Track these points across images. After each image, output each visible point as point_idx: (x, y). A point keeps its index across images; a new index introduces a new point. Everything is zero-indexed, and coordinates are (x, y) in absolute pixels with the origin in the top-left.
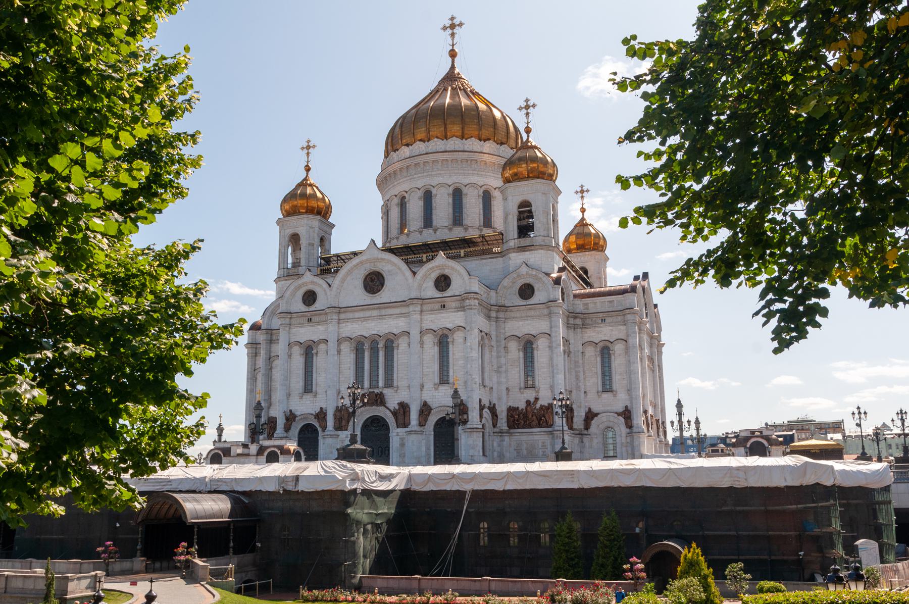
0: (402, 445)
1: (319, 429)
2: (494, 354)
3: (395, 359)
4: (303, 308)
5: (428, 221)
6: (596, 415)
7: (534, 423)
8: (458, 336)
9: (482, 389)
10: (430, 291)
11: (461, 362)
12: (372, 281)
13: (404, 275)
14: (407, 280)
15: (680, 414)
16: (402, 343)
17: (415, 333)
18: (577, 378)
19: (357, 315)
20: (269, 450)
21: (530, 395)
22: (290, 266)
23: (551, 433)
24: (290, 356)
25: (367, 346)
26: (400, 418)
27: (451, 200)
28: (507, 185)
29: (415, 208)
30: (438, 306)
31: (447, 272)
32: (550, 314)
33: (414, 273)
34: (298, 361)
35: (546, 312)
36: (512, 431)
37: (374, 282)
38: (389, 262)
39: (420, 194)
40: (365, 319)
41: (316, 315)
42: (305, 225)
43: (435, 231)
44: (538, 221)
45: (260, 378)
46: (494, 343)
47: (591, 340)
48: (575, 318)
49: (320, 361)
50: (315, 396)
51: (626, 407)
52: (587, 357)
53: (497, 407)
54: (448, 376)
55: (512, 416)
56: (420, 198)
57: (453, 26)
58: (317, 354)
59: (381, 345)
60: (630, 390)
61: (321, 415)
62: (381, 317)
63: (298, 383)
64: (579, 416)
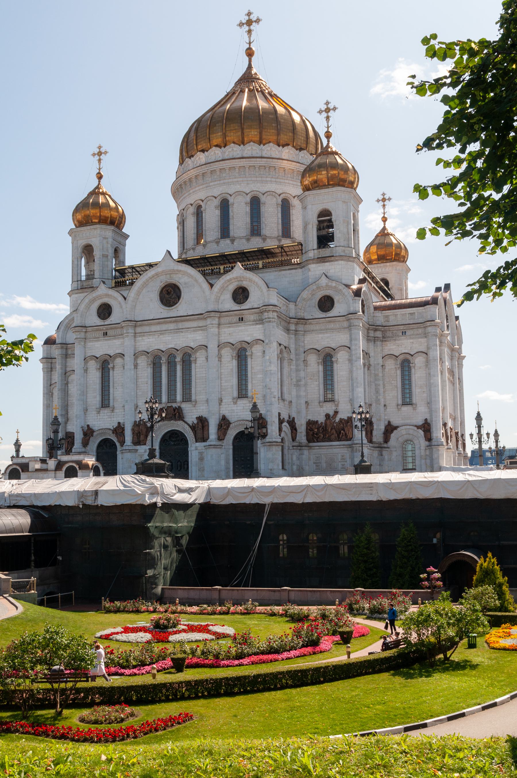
0: (201, 459)
1: (118, 444)
2: (293, 367)
3: (193, 373)
4: (98, 321)
5: (225, 231)
7: (333, 437)
8: (257, 350)
9: (281, 403)
10: (228, 303)
11: (260, 376)
12: (168, 293)
13: (201, 287)
14: (204, 292)
15: (479, 427)
16: (200, 358)
17: (213, 347)
18: (377, 392)
19: (154, 328)
20: (67, 465)
21: (329, 408)
22: (83, 278)
23: (351, 446)
24: (86, 370)
25: (164, 360)
26: (199, 432)
27: (248, 209)
28: (307, 193)
29: (212, 217)
30: (236, 319)
31: (245, 284)
32: (350, 327)
33: (212, 285)
34: (94, 375)
35: (346, 324)
36: (311, 444)
37: (170, 295)
38: (185, 273)
39: (217, 202)
40: (162, 332)
41: (112, 329)
42: (98, 236)
43: (233, 241)
44: (338, 231)
45: (56, 393)
46: (293, 356)
47: (391, 353)
48: (376, 330)
49: (117, 376)
50: (113, 411)
51: (426, 420)
52: (387, 370)
53: (296, 421)
54: (246, 390)
55: (311, 430)
56: (216, 207)
58: (113, 368)
59: (178, 359)
60: (430, 404)
61: (119, 430)
62: (178, 330)
63: (94, 398)
64: (379, 429)
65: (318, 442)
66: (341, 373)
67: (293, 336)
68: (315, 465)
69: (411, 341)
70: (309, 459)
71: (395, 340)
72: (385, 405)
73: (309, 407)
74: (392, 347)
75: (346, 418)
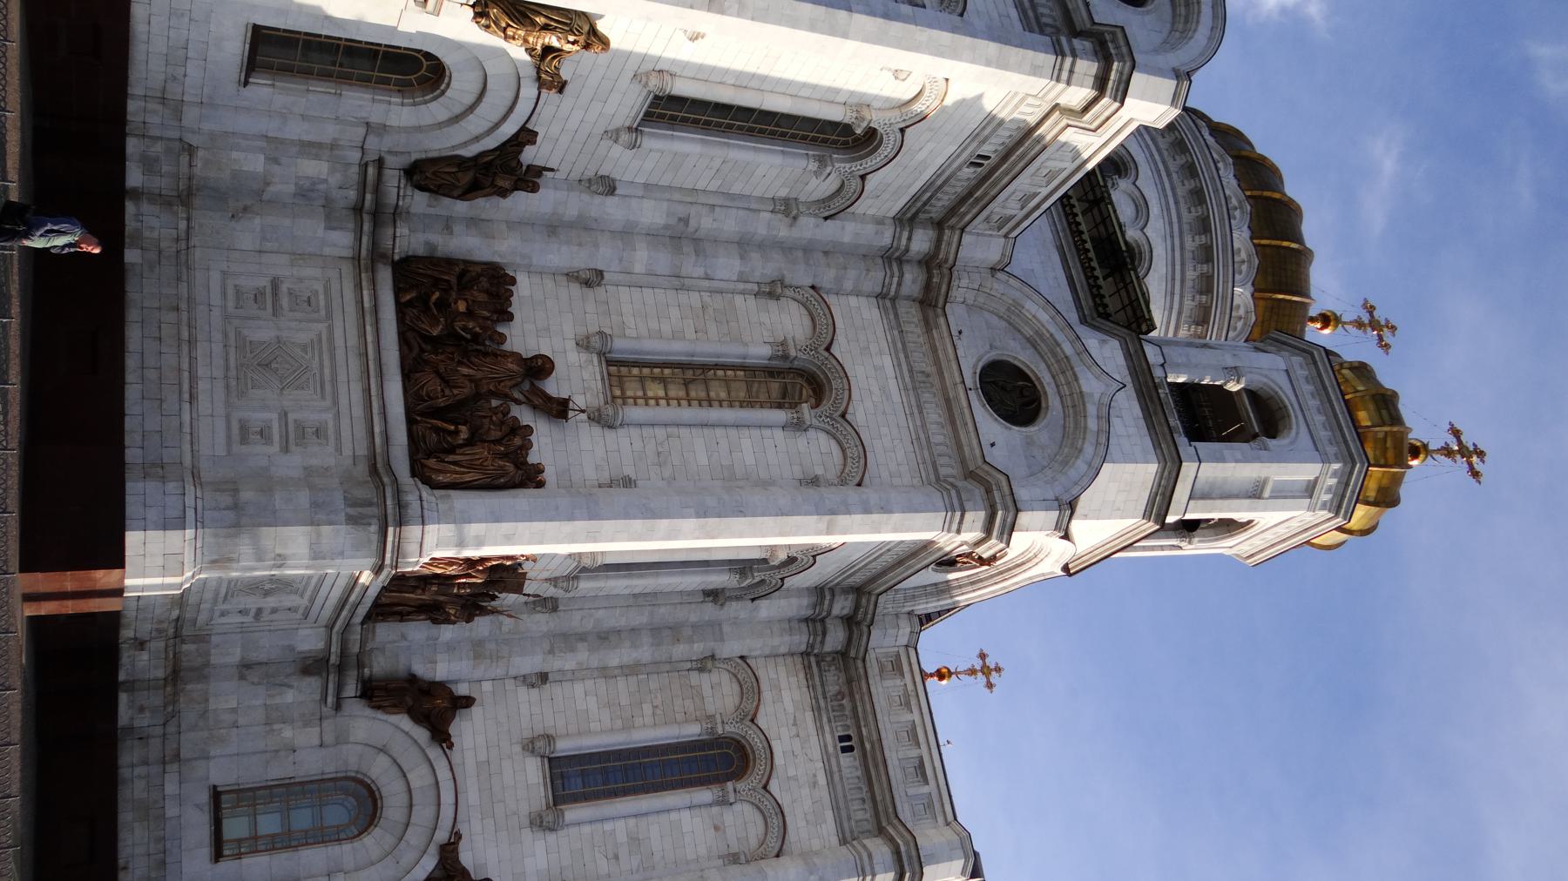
2: (765, 224)
6: (442, 737)
7: (431, 384)
18: (604, 637)
21: (576, 377)
35: (949, 469)
36: (385, 276)
46: (809, 228)
47: (767, 695)
48: (850, 621)
52: (695, 677)
53: (520, 202)
57: (1374, 324)
64: (434, 650)
65: (401, 309)
66: (746, 443)
67: (886, 239)
68: (264, 282)
69: (822, 780)
70: (298, 257)
71: (817, 709)
72: (543, 677)
73: (575, 288)
74: (786, 695)
75: (532, 458)
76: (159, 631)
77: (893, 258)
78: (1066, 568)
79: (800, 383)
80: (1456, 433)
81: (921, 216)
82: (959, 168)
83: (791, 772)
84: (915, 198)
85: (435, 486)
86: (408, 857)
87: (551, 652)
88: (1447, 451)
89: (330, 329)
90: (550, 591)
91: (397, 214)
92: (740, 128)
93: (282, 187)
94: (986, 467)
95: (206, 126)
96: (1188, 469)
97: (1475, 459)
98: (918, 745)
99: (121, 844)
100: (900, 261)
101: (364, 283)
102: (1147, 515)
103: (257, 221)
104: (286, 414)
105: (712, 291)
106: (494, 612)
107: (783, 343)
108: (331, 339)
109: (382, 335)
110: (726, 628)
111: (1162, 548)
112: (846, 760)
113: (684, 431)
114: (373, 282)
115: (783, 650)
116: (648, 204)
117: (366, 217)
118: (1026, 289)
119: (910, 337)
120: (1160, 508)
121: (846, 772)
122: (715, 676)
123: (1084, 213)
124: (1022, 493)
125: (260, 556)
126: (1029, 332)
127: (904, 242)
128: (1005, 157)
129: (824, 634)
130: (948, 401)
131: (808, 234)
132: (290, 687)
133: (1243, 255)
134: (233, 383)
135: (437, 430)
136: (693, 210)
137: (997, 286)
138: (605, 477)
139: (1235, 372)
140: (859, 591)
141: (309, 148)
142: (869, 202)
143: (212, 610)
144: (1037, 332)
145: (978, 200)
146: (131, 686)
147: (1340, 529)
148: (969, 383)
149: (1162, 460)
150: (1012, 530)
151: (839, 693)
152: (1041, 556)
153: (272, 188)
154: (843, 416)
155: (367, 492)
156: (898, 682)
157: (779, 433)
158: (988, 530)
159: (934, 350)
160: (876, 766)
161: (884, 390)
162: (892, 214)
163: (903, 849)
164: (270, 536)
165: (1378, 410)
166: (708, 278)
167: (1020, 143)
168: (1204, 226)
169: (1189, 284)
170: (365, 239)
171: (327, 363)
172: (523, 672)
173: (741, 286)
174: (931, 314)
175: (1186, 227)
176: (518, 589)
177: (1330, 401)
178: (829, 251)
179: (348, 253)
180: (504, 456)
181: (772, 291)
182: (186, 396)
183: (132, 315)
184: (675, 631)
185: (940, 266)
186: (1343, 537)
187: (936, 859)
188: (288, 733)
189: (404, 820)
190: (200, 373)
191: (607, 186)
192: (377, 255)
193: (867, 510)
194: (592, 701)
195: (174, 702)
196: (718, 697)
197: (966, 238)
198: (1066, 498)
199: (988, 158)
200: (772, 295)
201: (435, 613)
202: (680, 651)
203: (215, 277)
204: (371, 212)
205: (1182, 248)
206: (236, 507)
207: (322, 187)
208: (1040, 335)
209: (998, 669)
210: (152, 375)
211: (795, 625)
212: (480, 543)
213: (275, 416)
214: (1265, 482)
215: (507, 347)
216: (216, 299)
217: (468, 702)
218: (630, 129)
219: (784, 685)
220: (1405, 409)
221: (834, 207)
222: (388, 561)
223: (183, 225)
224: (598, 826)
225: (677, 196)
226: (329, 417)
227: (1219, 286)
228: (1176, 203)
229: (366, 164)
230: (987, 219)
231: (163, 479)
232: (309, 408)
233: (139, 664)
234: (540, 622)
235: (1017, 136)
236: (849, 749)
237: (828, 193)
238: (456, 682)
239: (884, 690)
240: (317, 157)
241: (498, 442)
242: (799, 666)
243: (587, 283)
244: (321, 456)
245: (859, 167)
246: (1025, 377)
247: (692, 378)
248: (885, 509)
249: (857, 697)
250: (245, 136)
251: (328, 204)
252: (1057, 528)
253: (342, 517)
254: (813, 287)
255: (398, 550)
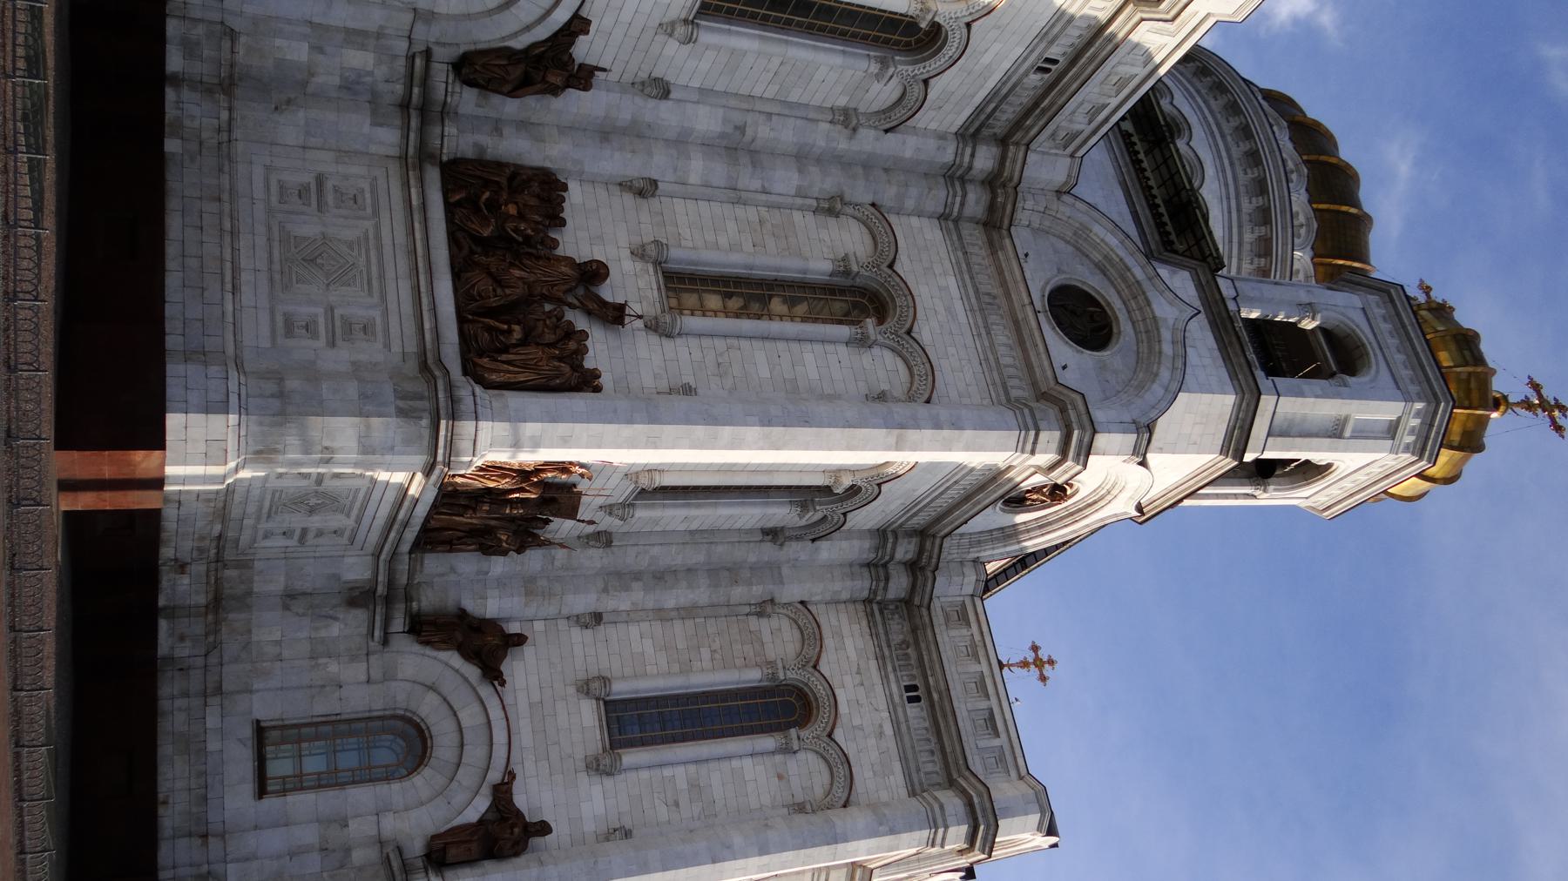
2: (823, 136)
7: (483, 284)
18: (661, 577)
21: (630, 283)
36: (433, 176)
46: (869, 141)
47: (829, 642)
48: (914, 567)
53: (574, 103)
64: (484, 585)
66: (809, 357)
67: (948, 156)
68: (308, 178)
69: (888, 730)
70: (343, 154)
71: (881, 658)
72: (598, 618)
73: (628, 198)
74: (849, 642)
75: (589, 363)
76: (201, 550)
77: (955, 176)
78: (1139, 508)
79: (861, 300)
80: (1536, 387)
81: (985, 132)
82: (1026, 74)
83: (856, 722)
84: (979, 110)
85: (488, 386)
86: (459, 798)
87: (605, 590)
88: (1527, 404)
89: (377, 227)
90: (607, 522)
91: (445, 113)
92: (799, 24)
93: (326, 79)
94: (1060, 389)
95: (249, 9)
96: (1267, 402)
97: (1556, 413)
98: (987, 696)
99: (160, 778)
100: (962, 180)
101: (412, 182)
102: (1224, 451)
103: (301, 114)
104: (332, 310)
105: (770, 206)
106: (547, 543)
107: (845, 259)
108: (378, 237)
109: (431, 234)
110: (785, 571)
111: (1236, 496)
112: (913, 710)
113: (744, 344)
114: (421, 181)
115: (845, 596)
116: (703, 110)
117: (414, 113)
118: (1095, 214)
119: (974, 259)
120: (1238, 442)
121: (914, 723)
122: (774, 622)
123: (1146, 154)
124: (1099, 415)
125: (307, 448)
126: (1097, 257)
127: (967, 159)
128: (1073, 62)
129: (887, 579)
130: (1016, 323)
131: (868, 148)
132: (336, 619)
133: (1302, 219)
134: (277, 277)
135: (489, 329)
136: (750, 118)
137: (1064, 209)
138: (664, 385)
139: (1310, 309)
140: (923, 534)
141: (355, 37)
142: (932, 114)
143: (255, 528)
144: (1106, 257)
145: (1044, 111)
146: (172, 612)
147: (1420, 476)
148: (1038, 306)
149: (1240, 391)
150: (1088, 454)
151: (904, 642)
152: (1114, 492)
153: (315, 80)
154: (909, 332)
155: (421, 387)
156: (964, 632)
157: (842, 349)
158: (1063, 452)
159: (1000, 272)
160: (945, 716)
161: (949, 310)
162: (954, 129)
163: (976, 800)
164: (317, 425)
165: (1460, 349)
166: (765, 192)
167: (1090, 43)
168: (1261, 187)
169: (1247, 247)
170: (412, 136)
171: (374, 260)
172: (575, 612)
173: (799, 201)
174: (995, 236)
175: (1242, 189)
176: (571, 513)
177: (1410, 340)
178: (891, 167)
179: (395, 152)
180: (560, 359)
181: (831, 208)
182: (229, 287)
183: (173, 204)
184: (730, 572)
185: (1004, 186)
186: (1425, 485)
187: (1011, 813)
188: (333, 667)
189: (455, 760)
190: (243, 263)
191: (661, 89)
192: (425, 156)
193: (938, 426)
194: (648, 643)
195: (217, 632)
196: (779, 642)
197: (1032, 157)
198: (1144, 421)
199: (1055, 62)
200: (832, 212)
201: (485, 542)
202: (738, 593)
203: (258, 173)
204: (418, 108)
205: (1239, 210)
206: (281, 395)
207: (368, 79)
208: (1110, 260)
209: (1051, 662)
210: (193, 263)
211: (856, 569)
212: (536, 444)
213: (320, 311)
214: (1346, 419)
215: (560, 252)
216: (259, 193)
217: (519, 640)
218: (686, 21)
219: (846, 630)
220: (1485, 347)
221: (895, 118)
222: (440, 458)
223: (225, 115)
224: (657, 772)
225: (733, 102)
226: (377, 314)
227: (1278, 248)
228: (1232, 164)
229: (413, 57)
230: (1053, 136)
231: (206, 364)
232: (356, 304)
233: (180, 589)
234: (594, 558)
235: (1088, 35)
236: (917, 699)
237: (889, 103)
238: (508, 620)
239: (950, 640)
240: (363, 47)
241: (549, 345)
242: (862, 614)
243: (641, 193)
244: (370, 352)
245: (921, 70)
246: (1098, 304)
247: (751, 294)
248: (957, 425)
249: (923, 645)
250: (289, 22)
251: (374, 100)
252: (1135, 452)
253: (392, 409)
254: (873, 205)
255: (450, 444)
